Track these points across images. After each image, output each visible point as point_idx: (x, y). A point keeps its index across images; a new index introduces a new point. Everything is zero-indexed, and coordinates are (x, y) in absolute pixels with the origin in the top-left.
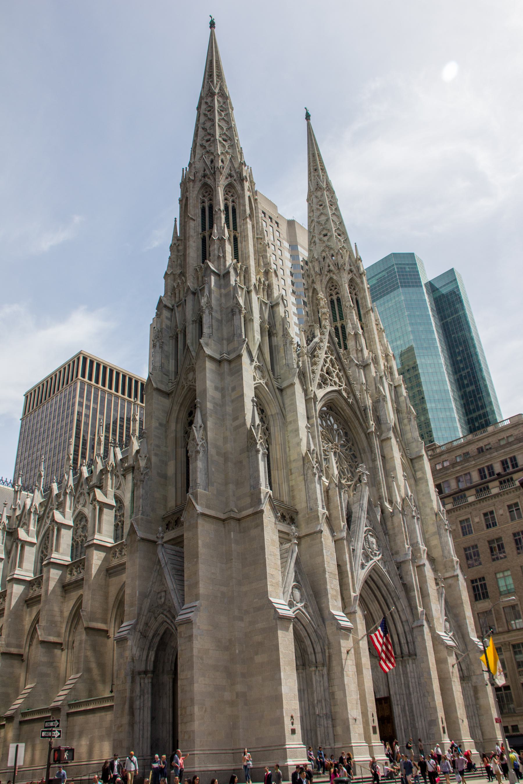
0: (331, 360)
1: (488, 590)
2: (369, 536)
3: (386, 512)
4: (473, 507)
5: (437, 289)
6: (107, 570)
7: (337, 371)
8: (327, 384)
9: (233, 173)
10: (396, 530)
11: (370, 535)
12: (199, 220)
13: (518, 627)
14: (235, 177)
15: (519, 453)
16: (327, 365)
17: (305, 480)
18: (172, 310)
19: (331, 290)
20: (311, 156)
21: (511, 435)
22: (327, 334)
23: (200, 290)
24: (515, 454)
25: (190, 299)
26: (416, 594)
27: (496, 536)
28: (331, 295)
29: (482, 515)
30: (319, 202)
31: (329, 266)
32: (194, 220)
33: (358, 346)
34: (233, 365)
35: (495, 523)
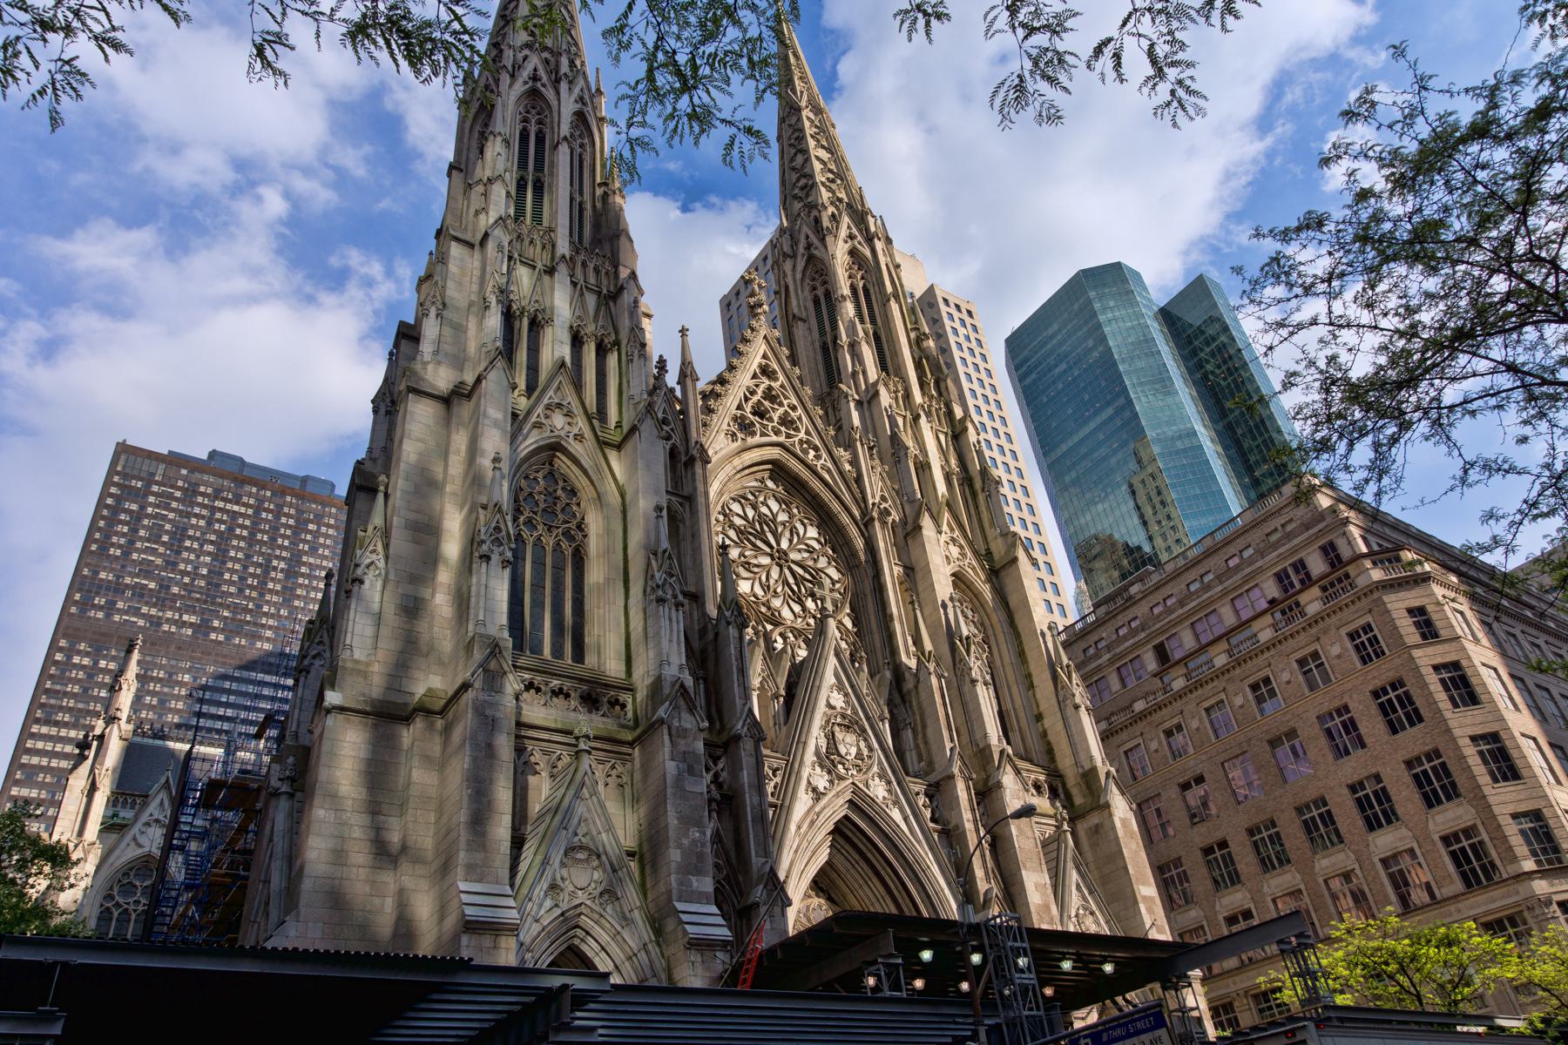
0: (770, 388)
1: (1287, 845)
2: (837, 728)
4: (1227, 676)
7: (781, 410)
8: (753, 434)
9: (542, 73)
11: (839, 725)
14: (545, 78)
15: (1310, 550)
16: (755, 398)
19: (814, 279)
21: (1291, 520)
24: (1302, 554)
27: (1284, 729)
28: (814, 288)
29: (1248, 690)
31: (807, 237)
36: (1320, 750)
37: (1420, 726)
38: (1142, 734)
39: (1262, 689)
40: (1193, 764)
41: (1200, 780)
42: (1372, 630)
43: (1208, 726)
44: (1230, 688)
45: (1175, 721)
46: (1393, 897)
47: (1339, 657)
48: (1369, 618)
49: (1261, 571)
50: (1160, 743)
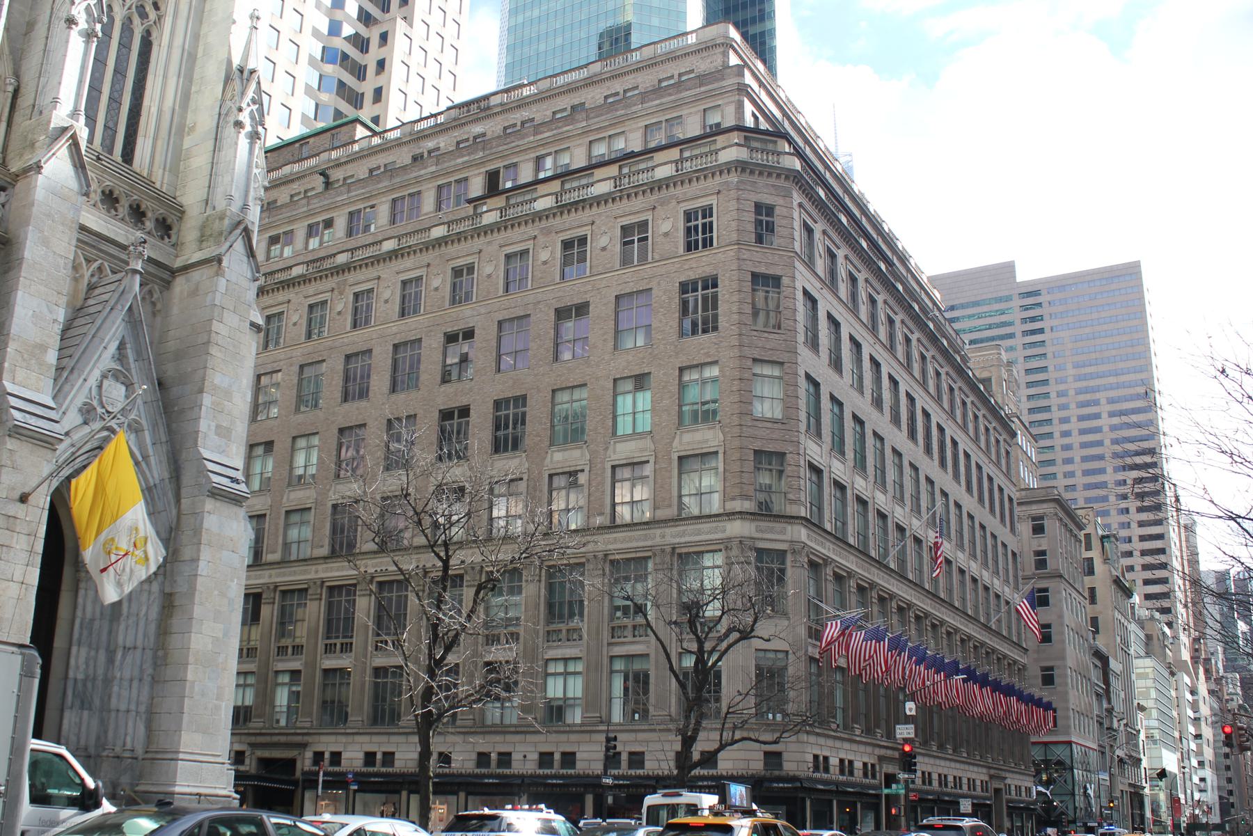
4: (544, 224)
15: (693, 110)
27: (577, 301)
36: (604, 334)
37: (712, 335)
38: (428, 265)
39: (574, 248)
40: (466, 315)
41: (469, 334)
42: (711, 216)
43: (502, 275)
44: (541, 240)
45: (469, 260)
47: (666, 234)
48: (713, 200)
50: (444, 281)
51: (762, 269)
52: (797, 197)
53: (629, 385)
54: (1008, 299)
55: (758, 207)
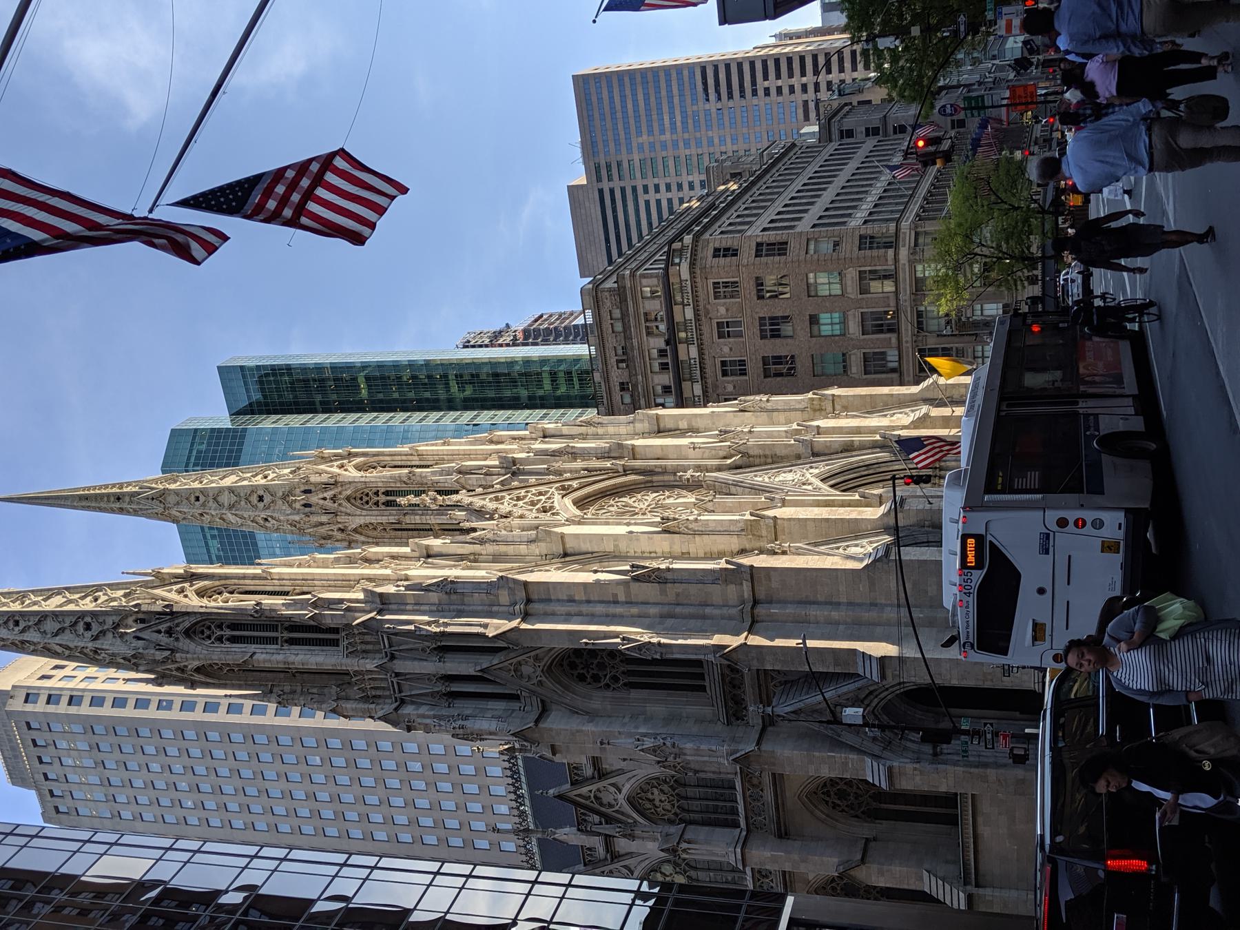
3: (739, 463)
4: (710, 390)
5: (251, 404)
6: (780, 837)
10: (767, 452)
12: (252, 648)
13: (897, 358)
14: (186, 585)
17: (702, 533)
18: (403, 702)
19: (367, 503)
20: (84, 503)
22: (471, 499)
23: (390, 647)
25: (401, 666)
26: (856, 438)
27: (761, 365)
28: (377, 504)
30: (190, 501)
31: (325, 499)
32: (254, 653)
33: (479, 472)
34: (534, 597)
35: (740, 361)
42: (719, 283)
44: (719, 391)
46: (888, 335)
47: (727, 310)
48: (711, 282)
49: (640, 345)
51: (753, 252)
52: (706, 236)
53: (815, 328)
54: (601, 191)
55: (714, 256)
